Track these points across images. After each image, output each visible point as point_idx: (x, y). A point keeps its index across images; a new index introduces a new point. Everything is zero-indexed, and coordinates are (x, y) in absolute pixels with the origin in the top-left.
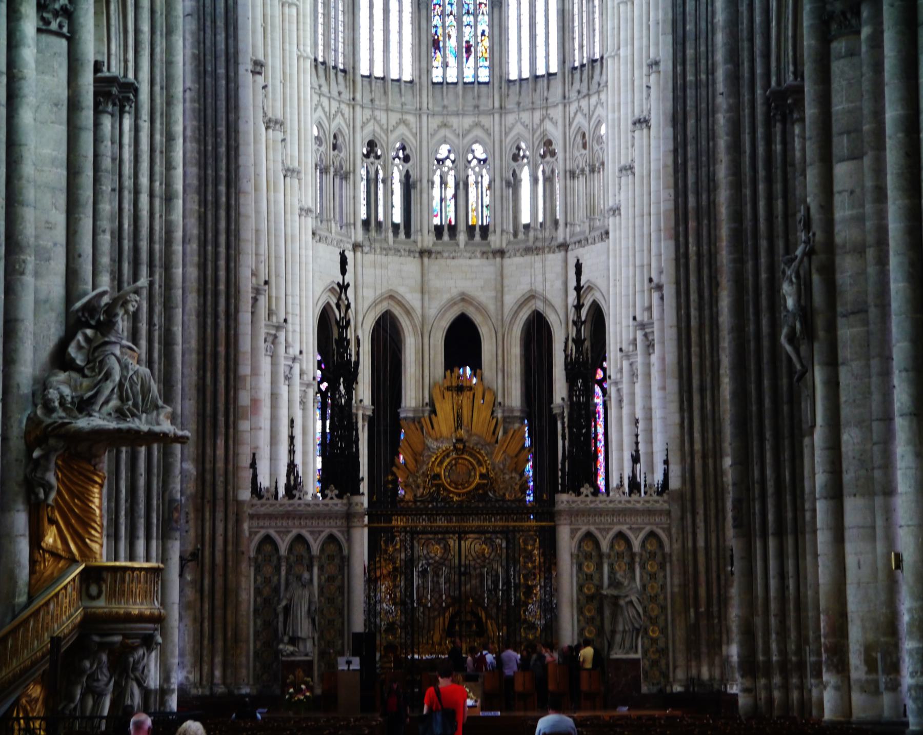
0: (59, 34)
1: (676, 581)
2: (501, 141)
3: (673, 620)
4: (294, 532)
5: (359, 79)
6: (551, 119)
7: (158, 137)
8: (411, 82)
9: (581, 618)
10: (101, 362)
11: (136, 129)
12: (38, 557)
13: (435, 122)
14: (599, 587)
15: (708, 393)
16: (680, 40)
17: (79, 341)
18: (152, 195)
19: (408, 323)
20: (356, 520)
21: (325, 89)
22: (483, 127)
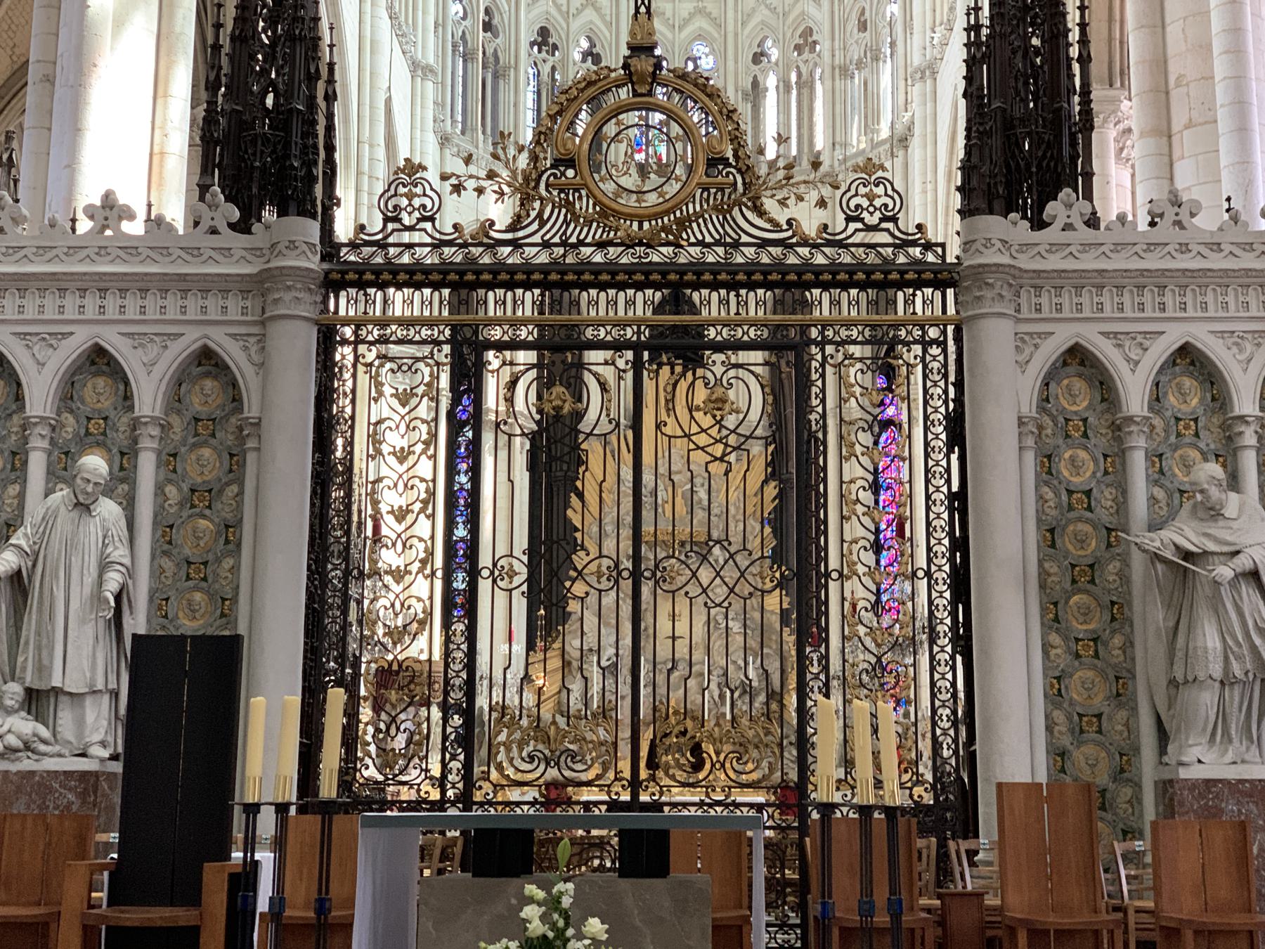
2: (736, 35)
4: (80, 340)
9: (1055, 639)
14: (1113, 534)
20: (287, 296)
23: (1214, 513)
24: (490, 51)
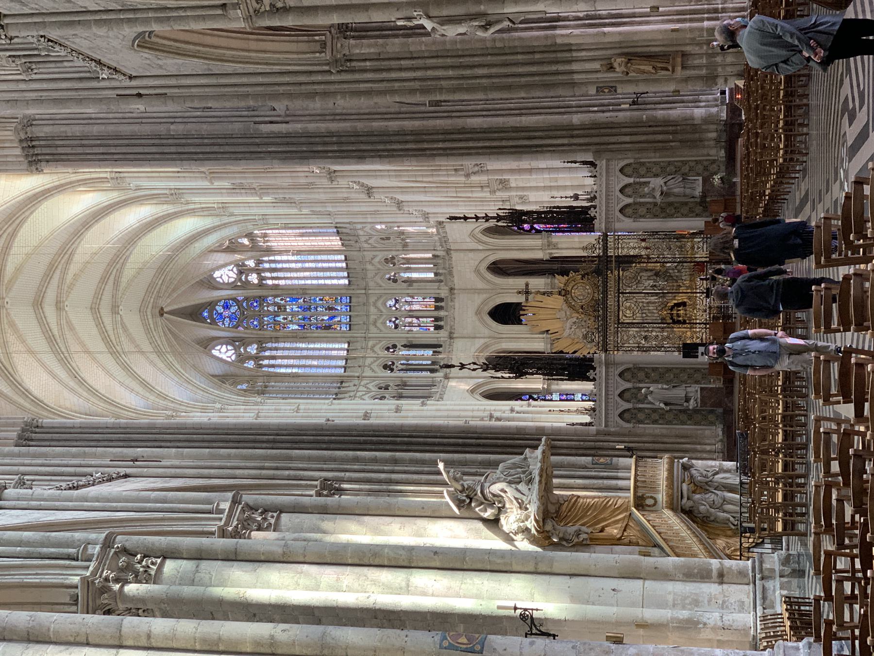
0: (278, 518)
1: (653, 155)
2: (385, 289)
3: (677, 156)
5: (346, 374)
6: (372, 259)
7: (355, 467)
8: (349, 343)
10: (494, 495)
11: (351, 481)
12: (626, 541)
13: (372, 329)
14: (655, 204)
15: (532, 134)
16: (312, 154)
17: (479, 510)
18: (393, 472)
19: (493, 346)
21: (352, 394)
22: (376, 301)
23: (654, 189)
24: (396, 388)
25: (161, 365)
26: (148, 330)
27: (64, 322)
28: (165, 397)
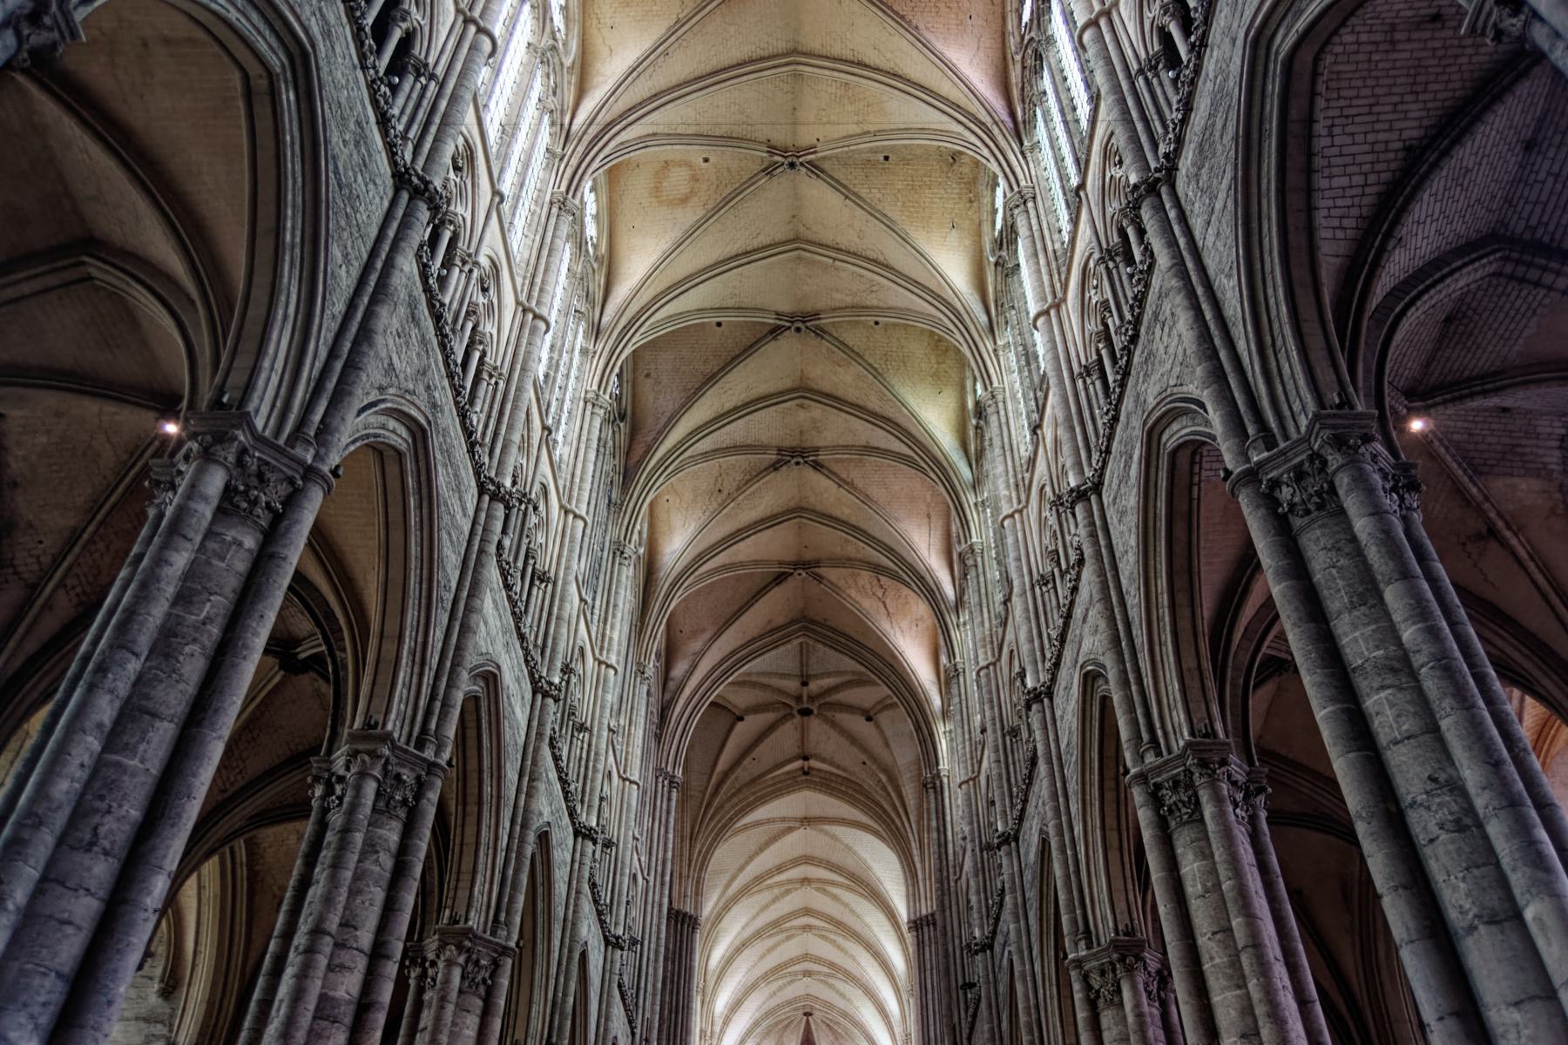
25: (758, 1015)
26: (789, 1003)
27: (793, 932)
28: (722, 1031)
